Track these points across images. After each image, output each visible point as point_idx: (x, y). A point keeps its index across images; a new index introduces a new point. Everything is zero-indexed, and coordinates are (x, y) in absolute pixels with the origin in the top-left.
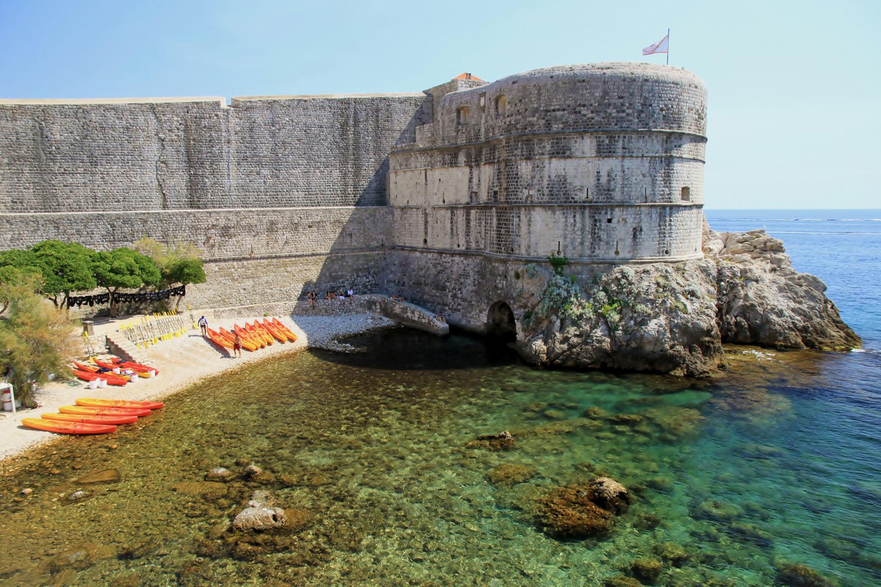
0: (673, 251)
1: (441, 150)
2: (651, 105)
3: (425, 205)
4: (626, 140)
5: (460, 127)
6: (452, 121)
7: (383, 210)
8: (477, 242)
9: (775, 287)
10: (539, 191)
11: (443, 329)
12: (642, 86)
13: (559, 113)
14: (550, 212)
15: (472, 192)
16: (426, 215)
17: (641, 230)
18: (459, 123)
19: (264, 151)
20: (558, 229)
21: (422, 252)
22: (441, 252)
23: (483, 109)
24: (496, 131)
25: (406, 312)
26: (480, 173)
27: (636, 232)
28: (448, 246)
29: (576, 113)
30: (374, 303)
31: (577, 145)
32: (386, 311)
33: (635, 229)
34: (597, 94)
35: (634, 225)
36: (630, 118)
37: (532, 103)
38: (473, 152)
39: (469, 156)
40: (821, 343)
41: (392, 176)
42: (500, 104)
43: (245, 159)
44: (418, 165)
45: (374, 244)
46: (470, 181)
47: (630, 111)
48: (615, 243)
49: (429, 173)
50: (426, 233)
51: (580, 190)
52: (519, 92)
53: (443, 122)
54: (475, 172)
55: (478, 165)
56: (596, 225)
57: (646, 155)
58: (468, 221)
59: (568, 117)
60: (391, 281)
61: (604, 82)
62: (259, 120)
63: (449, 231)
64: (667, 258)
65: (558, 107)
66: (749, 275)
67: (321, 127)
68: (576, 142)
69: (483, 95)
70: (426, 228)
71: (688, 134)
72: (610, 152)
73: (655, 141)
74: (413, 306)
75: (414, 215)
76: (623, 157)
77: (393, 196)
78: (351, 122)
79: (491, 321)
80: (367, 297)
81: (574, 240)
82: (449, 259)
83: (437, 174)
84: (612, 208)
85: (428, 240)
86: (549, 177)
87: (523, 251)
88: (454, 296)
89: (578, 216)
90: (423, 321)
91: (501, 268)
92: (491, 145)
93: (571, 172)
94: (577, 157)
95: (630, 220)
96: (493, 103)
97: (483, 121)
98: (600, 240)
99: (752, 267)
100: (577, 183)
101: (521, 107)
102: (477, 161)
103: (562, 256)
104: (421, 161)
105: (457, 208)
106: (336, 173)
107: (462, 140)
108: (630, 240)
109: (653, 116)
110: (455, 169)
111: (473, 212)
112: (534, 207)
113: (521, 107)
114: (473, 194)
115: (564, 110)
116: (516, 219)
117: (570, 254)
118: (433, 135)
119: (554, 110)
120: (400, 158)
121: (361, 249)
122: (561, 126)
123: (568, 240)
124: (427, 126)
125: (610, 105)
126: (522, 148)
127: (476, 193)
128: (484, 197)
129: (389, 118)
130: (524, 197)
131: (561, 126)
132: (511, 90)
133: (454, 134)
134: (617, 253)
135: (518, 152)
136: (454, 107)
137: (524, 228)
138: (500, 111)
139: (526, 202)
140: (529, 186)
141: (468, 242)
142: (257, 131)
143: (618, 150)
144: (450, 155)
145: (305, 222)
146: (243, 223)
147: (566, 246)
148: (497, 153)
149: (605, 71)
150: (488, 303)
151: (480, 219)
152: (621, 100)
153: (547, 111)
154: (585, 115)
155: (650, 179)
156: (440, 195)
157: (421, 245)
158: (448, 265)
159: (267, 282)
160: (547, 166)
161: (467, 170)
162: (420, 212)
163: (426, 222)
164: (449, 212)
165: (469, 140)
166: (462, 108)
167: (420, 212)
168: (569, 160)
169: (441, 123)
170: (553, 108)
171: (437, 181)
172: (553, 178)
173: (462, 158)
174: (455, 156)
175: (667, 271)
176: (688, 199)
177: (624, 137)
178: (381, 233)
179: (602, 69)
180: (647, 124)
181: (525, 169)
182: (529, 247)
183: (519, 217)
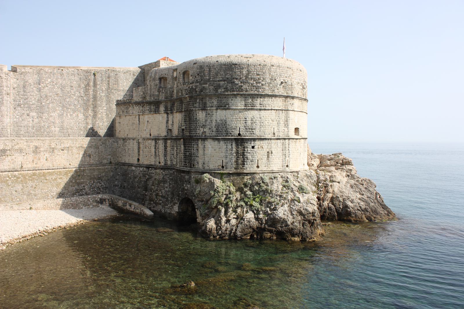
0: (291, 166)
1: (150, 103)
2: (275, 80)
4: (262, 99)
5: (161, 89)
6: (156, 85)
7: (111, 140)
8: (171, 160)
9: (349, 185)
10: (210, 129)
11: (151, 215)
12: (270, 68)
13: (222, 83)
14: (216, 142)
15: (168, 129)
17: (272, 153)
18: (160, 87)
19: (33, 101)
20: (222, 152)
21: (136, 167)
22: (148, 167)
24: (184, 92)
25: (126, 206)
26: (173, 117)
27: (269, 154)
28: (153, 163)
29: (232, 83)
30: (105, 200)
31: (233, 101)
32: (113, 205)
33: (268, 152)
34: (244, 72)
35: (268, 150)
36: (264, 86)
37: (205, 75)
40: (375, 218)
42: (186, 76)
43: (19, 105)
45: (105, 161)
47: (264, 83)
48: (257, 161)
49: (141, 117)
50: (139, 155)
53: (151, 86)
54: (170, 117)
55: (172, 113)
56: (244, 150)
57: (273, 108)
58: (166, 147)
59: (227, 85)
60: (116, 186)
61: (248, 65)
62: (30, 81)
63: (154, 154)
64: (287, 169)
65: (221, 79)
66: (334, 179)
67: (72, 87)
68: (232, 100)
69: (175, 70)
70: (139, 152)
71: (297, 97)
72: (252, 106)
73: (279, 100)
74: (130, 202)
75: (131, 145)
76: (260, 110)
77: (118, 131)
78: (92, 84)
79: (180, 210)
80: (100, 196)
82: (153, 171)
83: (146, 118)
84: (254, 140)
85: (140, 159)
86: (216, 121)
87: (200, 166)
88: (157, 195)
90: (137, 211)
91: (187, 177)
92: (181, 100)
95: (265, 147)
96: (182, 75)
97: (175, 86)
98: (248, 159)
99: (335, 174)
101: (198, 78)
102: (171, 110)
104: (136, 109)
105: (159, 139)
106: (81, 116)
107: (162, 97)
108: (266, 159)
109: (277, 86)
110: (158, 115)
111: (169, 141)
114: (170, 131)
115: (224, 81)
118: (144, 93)
119: (219, 81)
121: (97, 165)
122: (223, 90)
123: (228, 159)
124: (140, 88)
125: (252, 79)
126: (199, 103)
127: (171, 130)
128: (175, 132)
129: (117, 81)
130: (201, 133)
131: (223, 90)
132: (193, 68)
133: (157, 93)
134: (258, 167)
135: (197, 105)
136: (157, 77)
137: (201, 152)
138: (186, 81)
140: (204, 126)
141: (165, 160)
142: (29, 89)
143: (257, 105)
144: (154, 105)
145: (59, 147)
146: (16, 147)
147: (227, 163)
148: (184, 106)
149: (248, 59)
150: (179, 199)
151: (173, 146)
152: (258, 76)
154: (237, 85)
155: (276, 122)
156: (148, 131)
157: (136, 162)
158: (154, 175)
159: (32, 187)
161: (166, 115)
162: (135, 141)
163: (139, 148)
164: (154, 141)
165: (166, 98)
166: (163, 78)
168: (227, 111)
169: (149, 87)
170: (218, 79)
171: (146, 123)
172: (218, 121)
173: (162, 108)
175: (287, 178)
176: (298, 135)
177: (261, 98)
178: (109, 155)
179: (247, 58)
180: (273, 91)
181: (201, 115)
182: (204, 163)
183: (198, 145)
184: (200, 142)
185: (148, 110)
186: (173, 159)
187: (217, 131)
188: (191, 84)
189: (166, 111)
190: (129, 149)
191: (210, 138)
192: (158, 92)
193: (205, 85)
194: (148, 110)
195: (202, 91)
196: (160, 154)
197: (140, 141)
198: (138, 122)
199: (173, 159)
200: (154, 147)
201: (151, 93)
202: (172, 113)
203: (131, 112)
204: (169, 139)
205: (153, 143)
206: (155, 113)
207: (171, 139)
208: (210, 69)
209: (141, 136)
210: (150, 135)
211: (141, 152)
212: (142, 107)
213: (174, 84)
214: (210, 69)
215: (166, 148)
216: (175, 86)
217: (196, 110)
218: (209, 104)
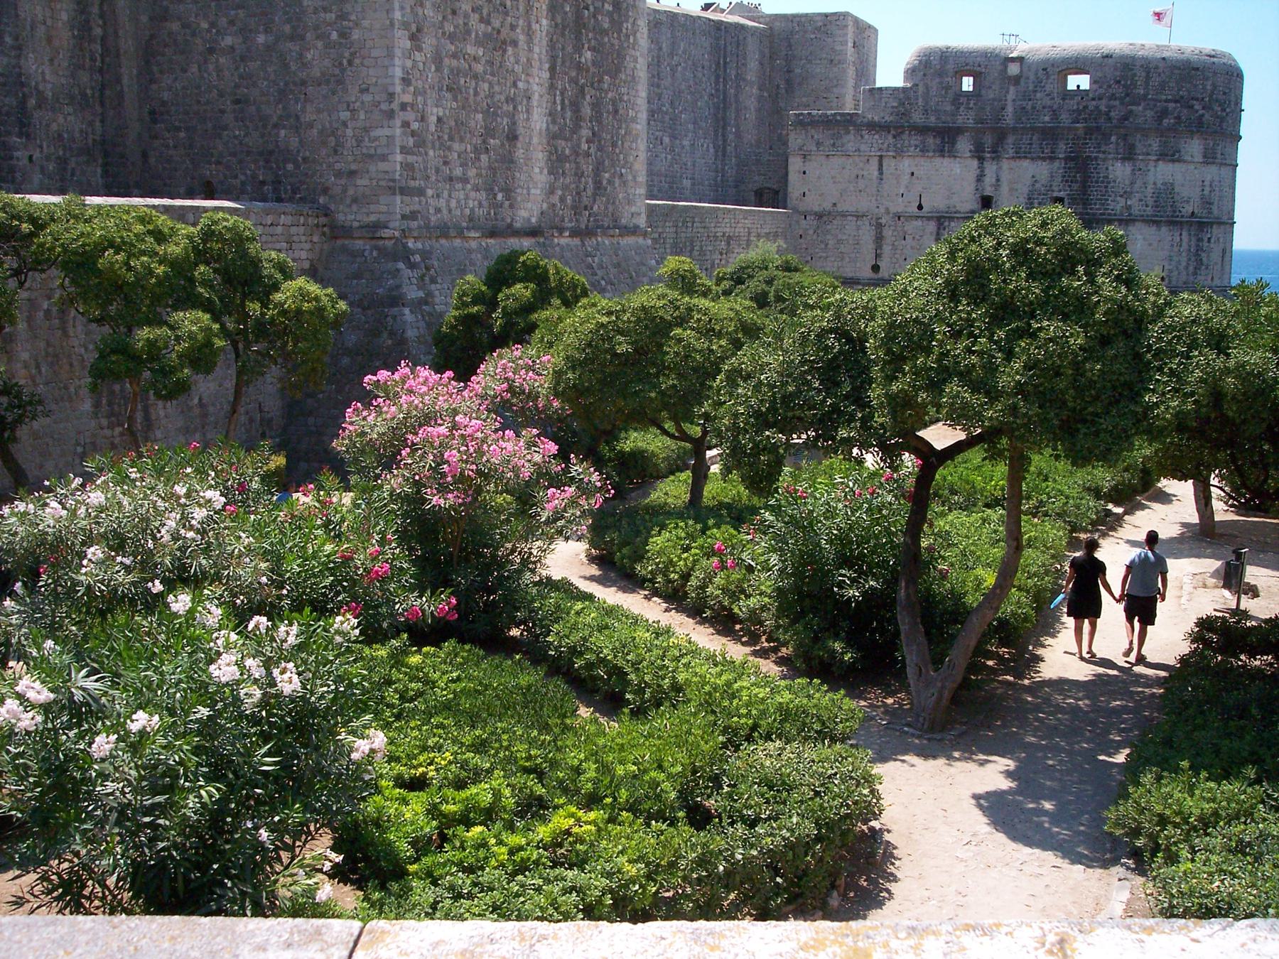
1: (923, 130)
10: (1141, 200)
13: (1172, 105)
14: (1154, 228)
16: (879, 226)
20: (1163, 249)
23: (1016, 80)
38: (988, 140)
41: (795, 164)
44: (863, 147)
46: (980, 178)
51: (1188, 202)
52: (1116, 69)
54: (990, 168)
76: (1221, 164)
84: (1212, 224)
85: (882, 264)
89: (1184, 233)
93: (1179, 177)
94: (1185, 162)
97: (1011, 96)
101: (1119, 91)
104: (873, 143)
105: (951, 219)
110: (946, 161)
112: (1134, 221)
113: (1119, 91)
115: (1176, 101)
119: (1166, 101)
126: (1117, 144)
133: (949, 108)
136: (950, 67)
157: (867, 273)
161: (975, 163)
163: (879, 239)
168: (1177, 165)
171: (907, 177)
174: (953, 143)
185: (916, 146)
187: (1157, 205)
188: (1093, 99)
189: (977, 151)
190: (840, 242)
191: (1143, 221)
192: (953, 104)
193: (1133, 108)
194: (916, 146)
195: (1126, 119)
197: (883, 221)
198: (876, 173)
201: (927, 103)
203: (850, 146)
205: (932, 226)
208: (1148, 73)
209: (887, 209)
210: (920, 207)
211: (887, 249)
212: (894, 137)
213: (1007, 92)
214: (1148, 73)
216: (1010, 97)
217: (1104, 160)
218: (1140, 148)
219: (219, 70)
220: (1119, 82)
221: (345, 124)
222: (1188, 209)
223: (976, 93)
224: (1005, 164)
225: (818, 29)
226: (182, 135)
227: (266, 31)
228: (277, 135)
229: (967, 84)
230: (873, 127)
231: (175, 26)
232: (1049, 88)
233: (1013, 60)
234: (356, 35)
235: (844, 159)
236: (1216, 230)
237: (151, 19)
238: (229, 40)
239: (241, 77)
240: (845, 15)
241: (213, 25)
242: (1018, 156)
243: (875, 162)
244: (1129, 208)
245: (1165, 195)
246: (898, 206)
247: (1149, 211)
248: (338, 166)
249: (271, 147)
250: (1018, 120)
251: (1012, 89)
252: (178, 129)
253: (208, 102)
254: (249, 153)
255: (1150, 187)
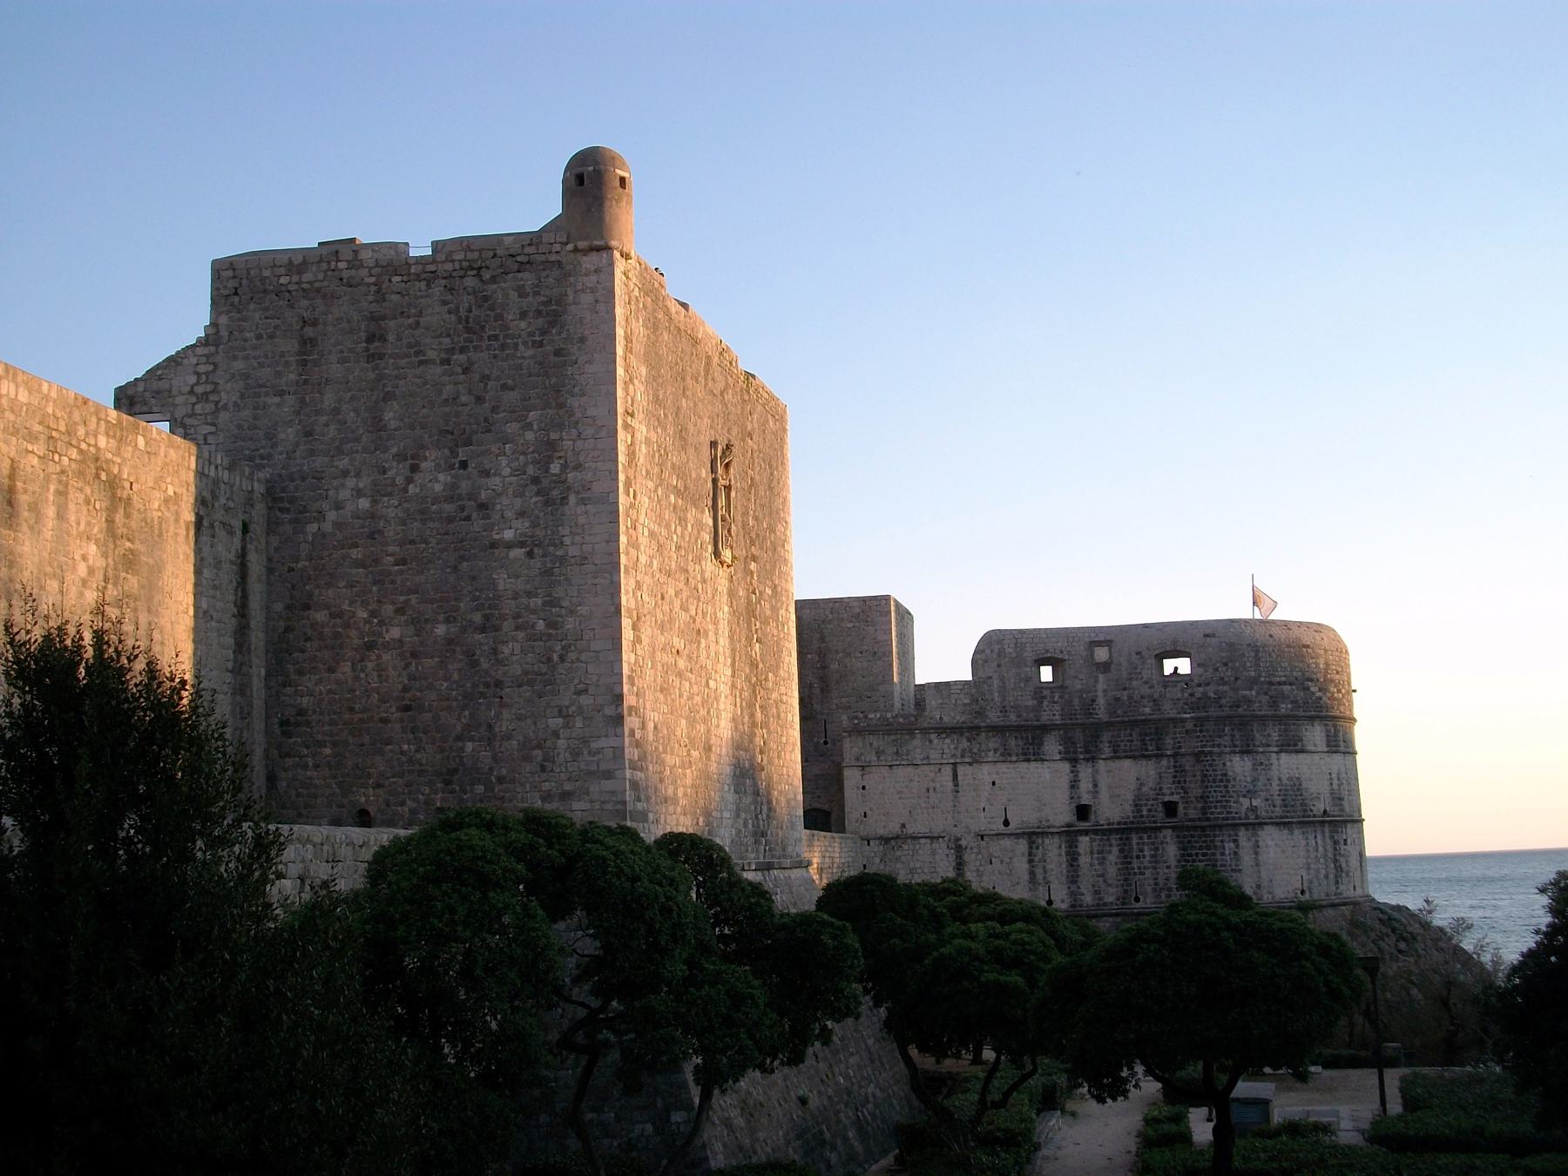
3: (958, 832)
8: (1097, 892)
16: (959, 850)
23: (1105, 667)
37: (1245, 668)
39: (1068, 742)
41: (851, 777)
44: (934, 755)
46: (1074, 784)
49: (961, 770)
53: (1002, 679)
58: (1073, 858)
63: (1026, 877)
81: (1318, 871)
100: (1313, 790)
103: (1307, 896)
105: (1044, 834)
110: (1033, 764)
111: (1084, 841)
112: (1261, 824)
114: (1083, 812)
116: (1230, 846)
117: (1318, 894)
120: (877, 742)
135: (1226, 740)
136: (1029, 655)
137: (1247, 858)
139: (1247, 817)
140: (1250, 794)
153: (1271, 683)
160: (1275, 762)
161: (1066, 767)
162: (942, 844)
167: (941, 847)
168: (1301, 756)
169: (996, 682)
171: (988, 787)
173: (1052, 746)
174: (1037, 742)
181: (1239, 767)
182: (1259, 887)
183: (1235, 841)
184: (1242, 832)
186: (1103, 887)
188: (1199, 685)
194: (996, 750)
196: (1051, 878)
197: (963, 843)
198: (951, 784)
199: (1103, 887)
200: (1025, 859)
202: (1092, 759)
204: (1086, 833)
205: (1023, 845)
206: (1029, 760)
207: (1096, 832)
208: (1257, 652)
210: (1006, 823)
212: (969, 740)
215: (1075, 860)
216: (1101, 686)
217: (1220, 754)
219: (380, 669)
220: (1226, 664)
221: (556, 734)
222: (1319, 807)
223: (1058, 685)
224: (1101, 765)
225: (857, 616)
226: (328, 751)
227: (447, 621)
228: (462, 749)
229: (1046, 674)
230: (944, 730)
231: (321, 616)
232: (1146, 674)
233: (1099, 644)
234: (570, 624)
235: (910, 769)
236: (1350, 829)
237: (288, 607)
238: (395, 633)
239: (412, 678)
240: (887, 598)
241: (373, 614)
242: (1116, 756)
243: (948, 770)
244: (1254, 809)
245: (1294, 792)
246: (981, 824)
247: (1278, 811)
248: (546, 786)
249: (453, 765)
250: (1113, 713)
251: (1101, 677)
252: (322, 744)
253: (365, 710)
254: (421, 773)
255: (1275, 783)
